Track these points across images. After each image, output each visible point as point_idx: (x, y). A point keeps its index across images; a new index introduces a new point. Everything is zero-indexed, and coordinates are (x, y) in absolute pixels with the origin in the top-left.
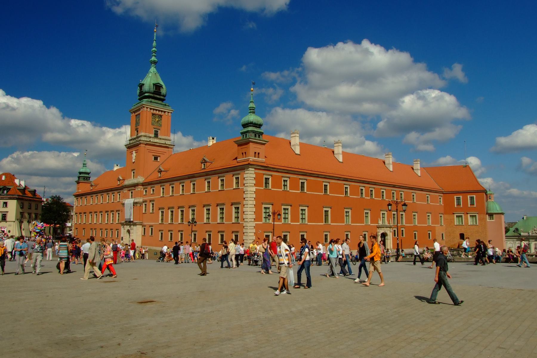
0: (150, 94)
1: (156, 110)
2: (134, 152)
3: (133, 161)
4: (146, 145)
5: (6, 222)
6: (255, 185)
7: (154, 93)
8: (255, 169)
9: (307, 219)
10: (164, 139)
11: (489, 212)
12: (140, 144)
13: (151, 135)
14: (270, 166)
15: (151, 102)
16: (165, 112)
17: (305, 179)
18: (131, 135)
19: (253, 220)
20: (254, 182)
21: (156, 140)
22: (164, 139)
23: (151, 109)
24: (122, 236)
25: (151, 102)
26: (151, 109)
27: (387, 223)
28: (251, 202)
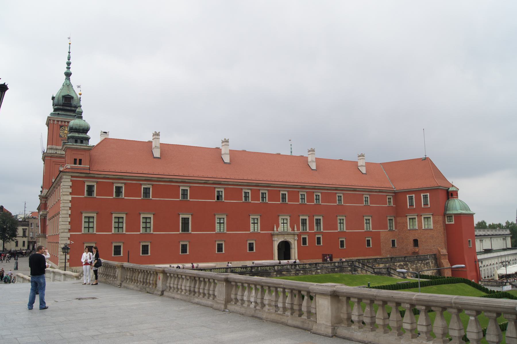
0: (59, 107)
1: (65, 122)
4: (51, 157)
6: (71, 194)
7: (63, 105)
8: (72, 177)
9: (152, 228)
11: (448, 212)
13: (58, 147)
14: (91, 172)
17: (149, 184)
19: (67, 231)
20: (70, 190)
26: (58, 121)
27: (290, 230)
28: (65, 212)
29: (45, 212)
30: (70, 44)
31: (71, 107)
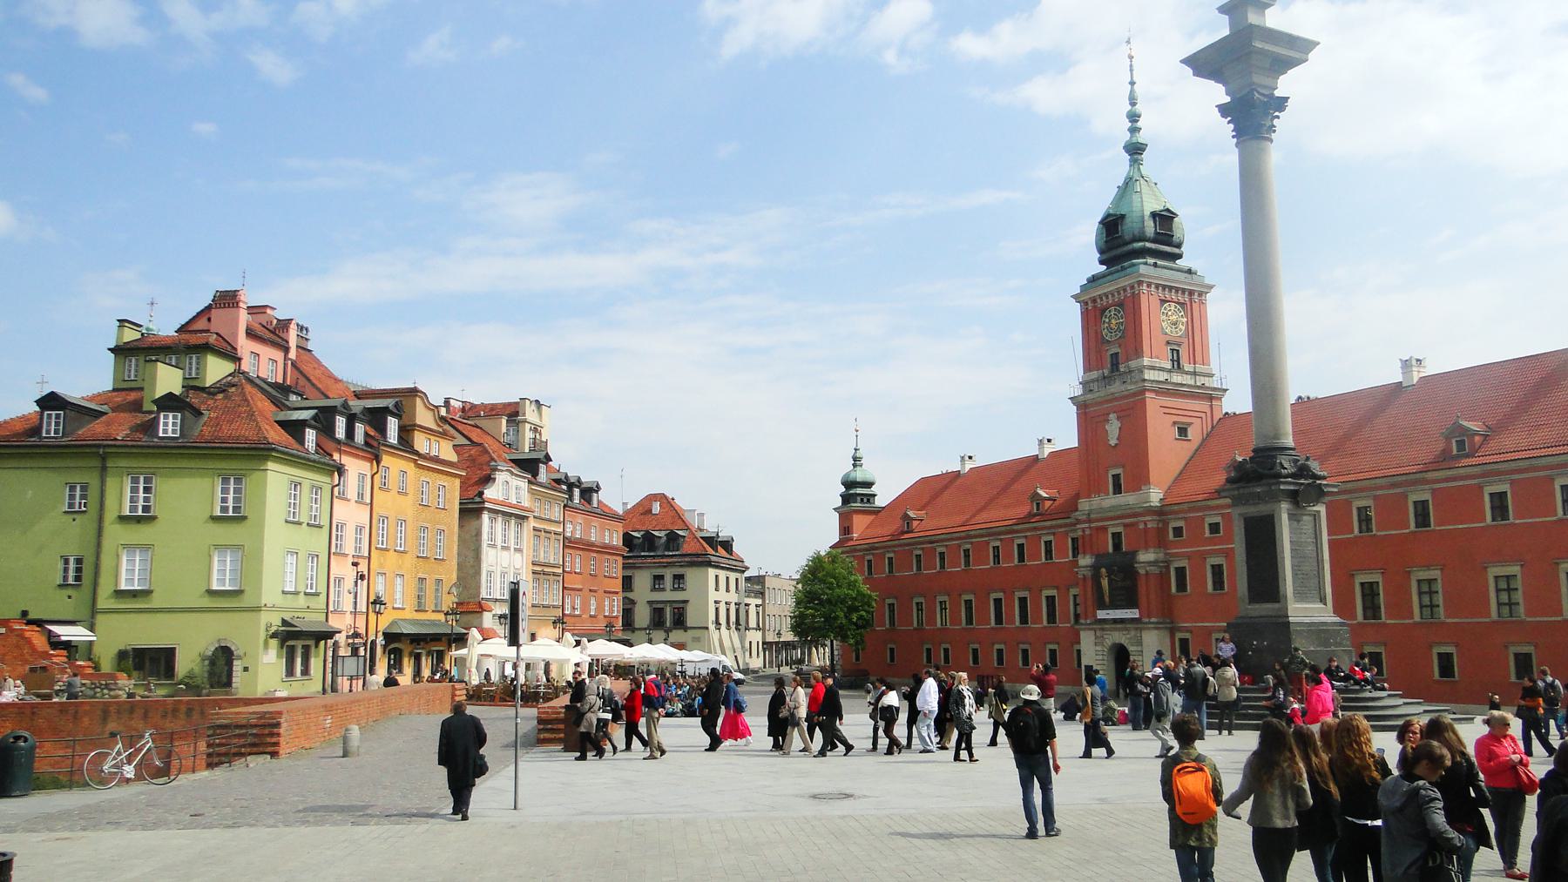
0: (1148, 245)
1: (1171, 288)
2: (1112, 416)
3: (1113, 442)
5: (686, 629)
10: (1195, 374)
12: (1143, 391)
15: (1155, 265)
16: (1191, 293)
18: (1088, 367)
21: (1177, 378)
22: (1195, 374)
23: (1157, 286)
24: (1085, 662)
25: (1155, 265)
26: (1157, 286)
29: (1161, 556)
30: (1131, 57)
31: (1169, 244)
